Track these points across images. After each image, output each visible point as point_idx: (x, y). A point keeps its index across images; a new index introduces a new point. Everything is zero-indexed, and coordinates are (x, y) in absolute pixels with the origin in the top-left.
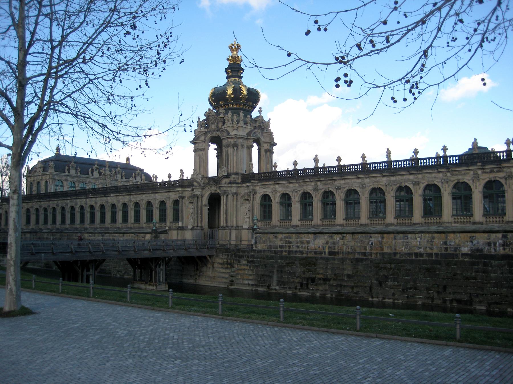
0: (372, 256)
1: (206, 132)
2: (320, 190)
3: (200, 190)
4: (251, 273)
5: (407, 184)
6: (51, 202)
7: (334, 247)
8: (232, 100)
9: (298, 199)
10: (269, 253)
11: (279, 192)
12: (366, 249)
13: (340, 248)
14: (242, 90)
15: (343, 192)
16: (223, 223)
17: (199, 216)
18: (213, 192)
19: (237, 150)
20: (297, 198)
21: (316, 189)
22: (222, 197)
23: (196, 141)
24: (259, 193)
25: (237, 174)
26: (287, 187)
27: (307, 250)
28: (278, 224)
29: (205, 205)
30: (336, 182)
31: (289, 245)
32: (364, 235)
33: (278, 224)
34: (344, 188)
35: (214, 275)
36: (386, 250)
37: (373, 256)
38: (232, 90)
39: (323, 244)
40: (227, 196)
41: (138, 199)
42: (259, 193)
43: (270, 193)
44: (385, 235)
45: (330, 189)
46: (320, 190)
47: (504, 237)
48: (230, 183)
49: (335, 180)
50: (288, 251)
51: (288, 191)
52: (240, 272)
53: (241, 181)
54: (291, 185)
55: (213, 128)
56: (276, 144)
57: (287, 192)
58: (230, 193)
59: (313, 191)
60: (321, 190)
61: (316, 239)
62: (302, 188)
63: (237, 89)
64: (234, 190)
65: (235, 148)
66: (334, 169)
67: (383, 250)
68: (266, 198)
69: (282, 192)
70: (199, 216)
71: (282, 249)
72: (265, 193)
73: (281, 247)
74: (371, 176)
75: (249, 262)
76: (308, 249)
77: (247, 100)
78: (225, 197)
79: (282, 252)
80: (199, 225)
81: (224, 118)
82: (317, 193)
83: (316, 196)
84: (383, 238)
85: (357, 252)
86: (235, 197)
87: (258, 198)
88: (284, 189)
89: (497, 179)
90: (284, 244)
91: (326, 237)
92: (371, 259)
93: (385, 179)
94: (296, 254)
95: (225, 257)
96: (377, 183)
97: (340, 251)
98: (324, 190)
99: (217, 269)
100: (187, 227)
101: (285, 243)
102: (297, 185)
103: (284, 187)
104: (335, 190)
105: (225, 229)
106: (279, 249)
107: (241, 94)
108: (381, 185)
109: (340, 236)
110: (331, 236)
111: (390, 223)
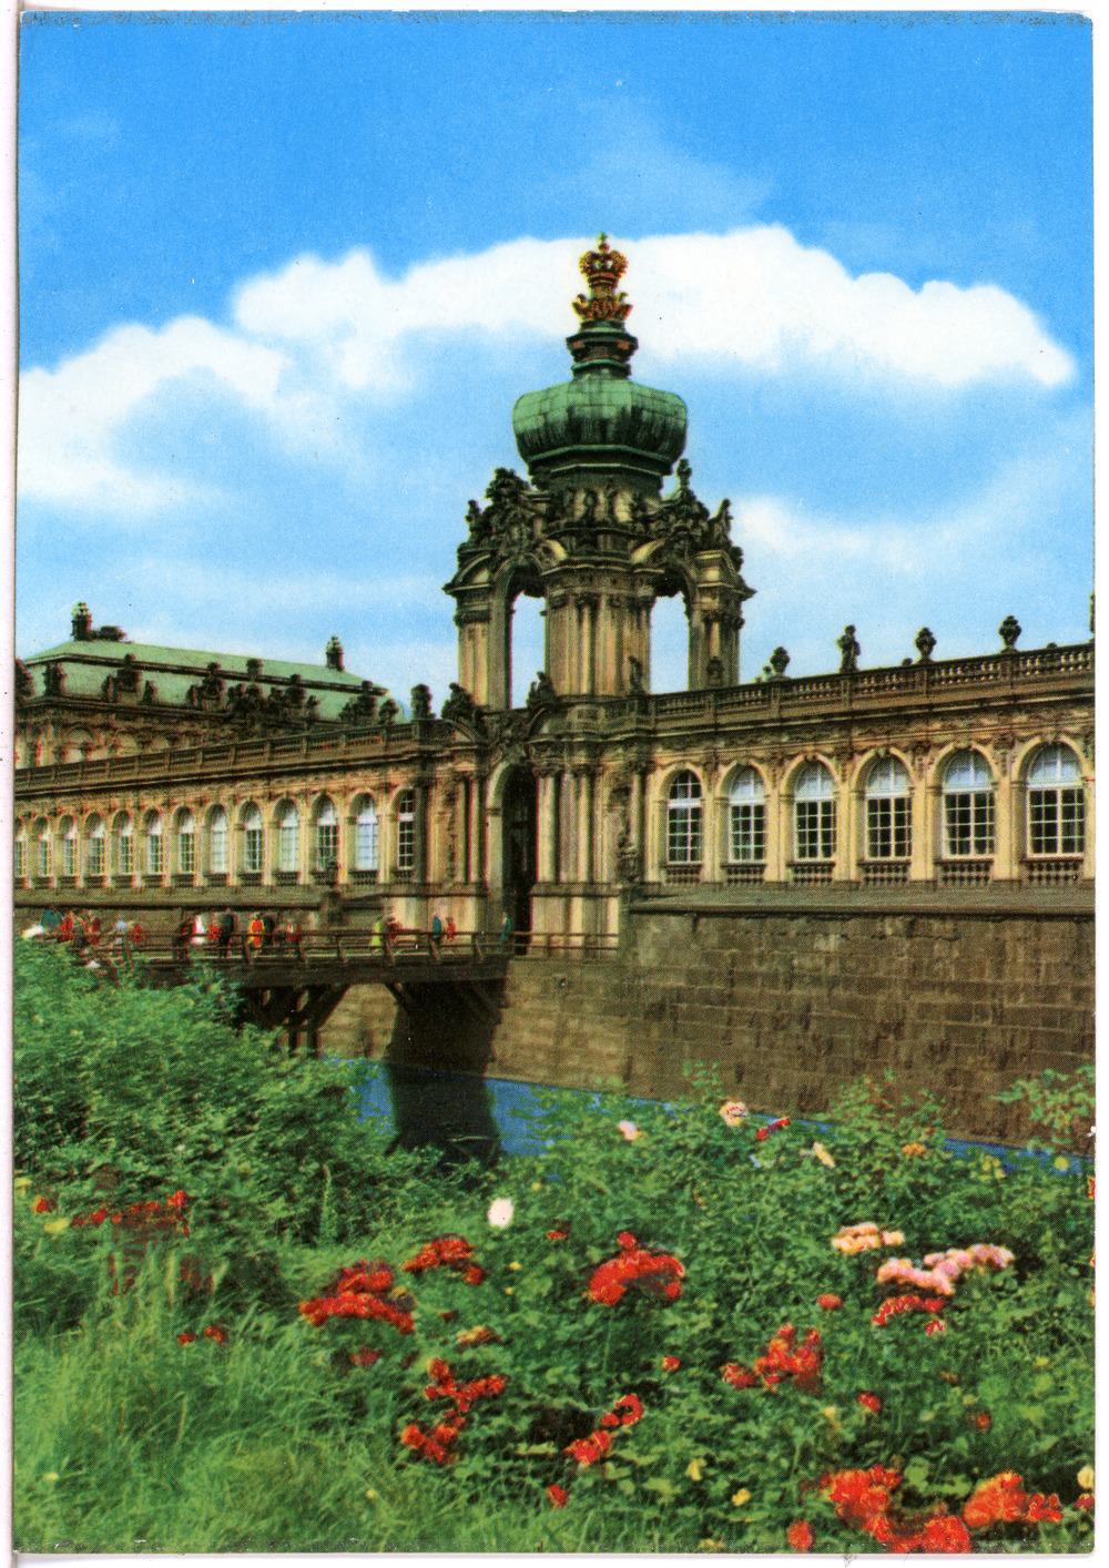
11: (727, 763)
16: (545, 871)
23: (464, 583)
29: (495, 812)
43: (696, 764)
56: (749, 593)
58: (568, 765)
65: (586, 611)
78: (550, 782)
80: (474, 877)
82: (849, 767)
86: (584, 781)
108: (1067, 733)
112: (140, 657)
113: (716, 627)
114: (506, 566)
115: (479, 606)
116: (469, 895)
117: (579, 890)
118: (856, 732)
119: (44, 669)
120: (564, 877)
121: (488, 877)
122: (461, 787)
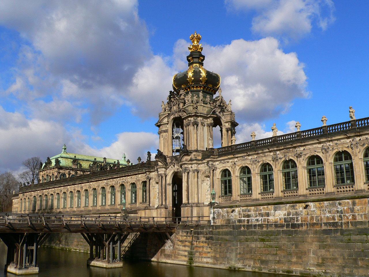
0: (342, 227)
1: (169, 114)
3: (164, 169)
4: (209, 250)
6: (50, 190)
7: (297, 218)
8: (192, 82)
9: (258, 171)
10: (227, 228)
12: (334, 218)
13: (303, 220)
14: (202, 73)
15: (305, 159)
16: (184, 200)
17: (164, 194)
18: (175, 171)
19: (197, 127)
20: (256, 170)
21: (275, 159)
22: (184, 175)
24: (219, 168)
25: (197, 151)
26: (247, 159)
27: (267, 223)
28: (239, 198)
29: (169, 184)
31: (247, 218)
32: (331, 202)
33: (239, 198)
34: (305, 155)
36: (359, 219)
37: (344, 226)
38: (192, 73)
39: (285, 215)
40: (188, 173)
41: (114, 183)
42: (219, 168)
43: (229, 167)
44: (357, 201)
45: (291, 158)
48: (191, 160)
50: (247, 225)
52: (201, 250)
53: (202, 158)
54: (250, 157)
55: (175, 109)
57: (246, 165)
59: (272, 161)
61: (276, 210)
63: (196, 72)
64: (194, 167)
65: (195, 126)
66: (294, 136)
67: (355, 219)
68: (226, 173)
69: (241, 166)
70: (164, 194)
71: (241, 224)
72: (225, 168)
73: (240, 221)
74: (334, 138)
75: (207, 239)
76: (268, 222)
77: (207, 82)
78: (186, 174)
79: (240, 226)
80: (164, 203)
81: (184, 99)
83: (276, 166)
84: (354, 204)
85: (324, 223)
86: (196, 173)
87: (218, 174)
90: (243, 218)
92: (342, 229)
94: (255, 229)
95: (185, 234)
96: (341, 146)
97: (304, 223)
98: (283, 159)
100: (154, 206)
101: (244, 217)
104: (296, 158)
105: (186, 207)
106: (237, 224)
107: (201, 76)
109: (304, 205)
110: (293, 206)
111: (360, 189)
112: (77, 158)
113: (230, 132)
114: (172, 117)
115: (163, 128)
116: (163, 208)
117: (195, 205)
118: (278, 152)
119: (55, 159)
120: (190, 201)
121: (167, 203)
122: (160, 178)
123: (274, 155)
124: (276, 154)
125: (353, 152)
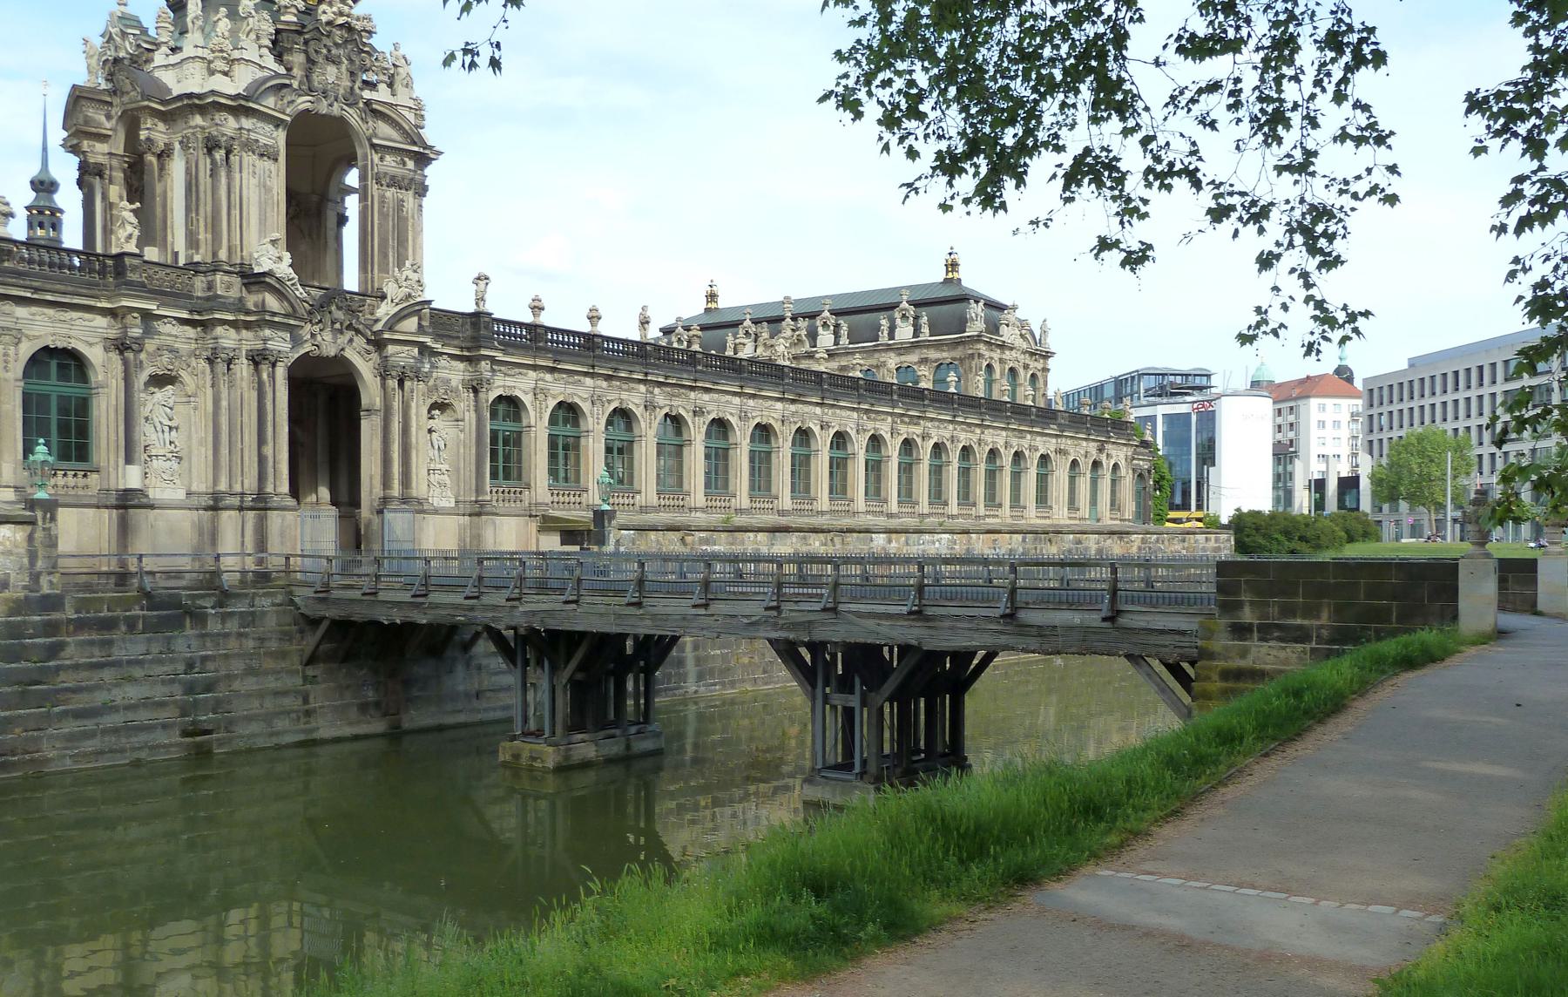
2: (658, 410)
5: (811, 425)
11: (554, 397)
21: (649, 406)
30: (692, 395)
34: (708, 413)
35: (476, 686)
44: (894, 536)
46: (658, 410)
47: (1024, 540)
49: (692, 388)
51: (580, 397)
54: (588, 381)
60: (661, 408)
61: (773, 544)
62: (617, 396)
69: (561, 398)
88: (570, 389)
89: (915, 437)
91: (794, 540)
93: (779, 405)
99: (484, 662)
102: (605, 384)
103: (569, 383)
104: (691, 414)
110: (805, 538)
118: (657, 390)
123: (647, 390)
124: (652, 393)
125: (782, 432)
